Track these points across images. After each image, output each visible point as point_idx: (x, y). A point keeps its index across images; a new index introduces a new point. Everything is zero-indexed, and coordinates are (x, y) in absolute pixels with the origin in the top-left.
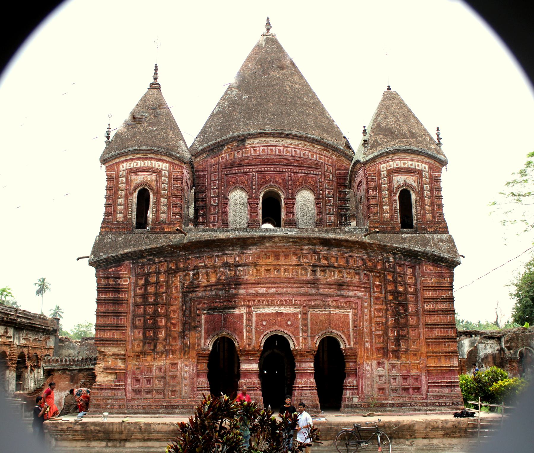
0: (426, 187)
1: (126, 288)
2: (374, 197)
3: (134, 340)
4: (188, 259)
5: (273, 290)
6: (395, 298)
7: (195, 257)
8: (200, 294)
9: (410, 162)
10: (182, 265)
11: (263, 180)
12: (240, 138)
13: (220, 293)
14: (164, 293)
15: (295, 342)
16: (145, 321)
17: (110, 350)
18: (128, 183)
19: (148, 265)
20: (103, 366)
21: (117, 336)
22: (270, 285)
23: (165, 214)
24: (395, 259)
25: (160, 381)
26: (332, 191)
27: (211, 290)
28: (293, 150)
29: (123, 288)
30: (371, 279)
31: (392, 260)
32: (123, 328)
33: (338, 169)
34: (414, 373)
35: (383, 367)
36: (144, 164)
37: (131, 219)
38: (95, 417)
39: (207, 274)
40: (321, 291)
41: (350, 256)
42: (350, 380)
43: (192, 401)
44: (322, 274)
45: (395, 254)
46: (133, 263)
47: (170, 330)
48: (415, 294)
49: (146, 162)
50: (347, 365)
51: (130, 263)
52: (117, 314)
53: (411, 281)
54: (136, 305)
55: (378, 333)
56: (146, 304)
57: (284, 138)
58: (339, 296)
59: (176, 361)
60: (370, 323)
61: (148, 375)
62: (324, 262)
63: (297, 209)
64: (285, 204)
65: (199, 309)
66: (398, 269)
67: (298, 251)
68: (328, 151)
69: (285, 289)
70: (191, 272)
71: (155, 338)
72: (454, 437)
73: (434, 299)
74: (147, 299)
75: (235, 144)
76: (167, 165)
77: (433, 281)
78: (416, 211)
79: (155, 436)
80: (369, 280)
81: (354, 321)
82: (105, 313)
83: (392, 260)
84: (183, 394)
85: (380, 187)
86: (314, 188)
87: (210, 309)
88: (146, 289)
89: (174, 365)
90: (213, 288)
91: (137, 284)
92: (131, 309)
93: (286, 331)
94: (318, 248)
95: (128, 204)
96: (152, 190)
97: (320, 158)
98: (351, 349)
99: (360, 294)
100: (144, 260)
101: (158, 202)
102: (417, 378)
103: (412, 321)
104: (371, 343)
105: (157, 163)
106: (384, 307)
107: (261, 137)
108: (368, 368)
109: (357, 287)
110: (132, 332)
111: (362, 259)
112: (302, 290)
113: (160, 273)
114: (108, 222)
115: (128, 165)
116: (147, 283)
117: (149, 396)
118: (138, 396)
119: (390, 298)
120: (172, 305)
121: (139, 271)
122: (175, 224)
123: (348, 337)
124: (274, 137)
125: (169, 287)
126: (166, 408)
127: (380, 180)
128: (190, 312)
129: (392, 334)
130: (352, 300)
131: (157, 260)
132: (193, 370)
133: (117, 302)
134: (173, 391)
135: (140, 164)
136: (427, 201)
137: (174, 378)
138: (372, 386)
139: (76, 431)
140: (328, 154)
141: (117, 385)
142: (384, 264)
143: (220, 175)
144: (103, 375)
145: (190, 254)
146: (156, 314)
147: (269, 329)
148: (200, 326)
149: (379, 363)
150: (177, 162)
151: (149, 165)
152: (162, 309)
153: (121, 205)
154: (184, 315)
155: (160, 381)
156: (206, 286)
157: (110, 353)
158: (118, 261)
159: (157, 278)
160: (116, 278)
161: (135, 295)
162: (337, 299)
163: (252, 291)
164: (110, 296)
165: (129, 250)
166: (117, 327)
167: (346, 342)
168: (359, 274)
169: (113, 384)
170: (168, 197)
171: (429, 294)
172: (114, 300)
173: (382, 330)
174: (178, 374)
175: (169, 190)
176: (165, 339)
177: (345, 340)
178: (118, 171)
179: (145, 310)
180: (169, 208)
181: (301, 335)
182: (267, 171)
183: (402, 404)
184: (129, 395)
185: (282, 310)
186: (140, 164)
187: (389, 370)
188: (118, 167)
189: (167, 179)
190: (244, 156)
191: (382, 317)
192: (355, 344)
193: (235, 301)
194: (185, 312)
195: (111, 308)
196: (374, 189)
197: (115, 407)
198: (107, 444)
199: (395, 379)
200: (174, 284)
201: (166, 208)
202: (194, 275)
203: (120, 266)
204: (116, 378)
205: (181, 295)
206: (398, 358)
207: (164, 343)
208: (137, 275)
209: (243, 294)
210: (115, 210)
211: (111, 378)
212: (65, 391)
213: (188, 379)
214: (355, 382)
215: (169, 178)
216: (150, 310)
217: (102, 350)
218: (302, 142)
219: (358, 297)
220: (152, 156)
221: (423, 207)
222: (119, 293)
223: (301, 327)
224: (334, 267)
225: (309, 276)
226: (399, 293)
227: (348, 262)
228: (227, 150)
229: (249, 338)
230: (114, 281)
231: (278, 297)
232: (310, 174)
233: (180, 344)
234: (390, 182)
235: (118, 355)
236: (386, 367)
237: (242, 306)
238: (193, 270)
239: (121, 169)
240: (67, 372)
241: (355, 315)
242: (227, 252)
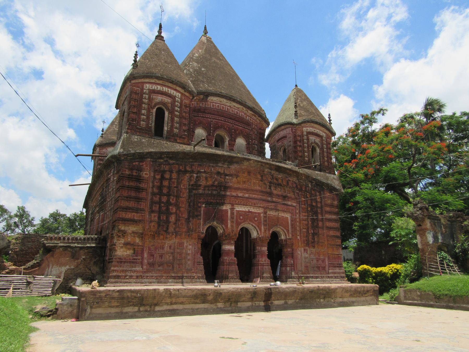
0: (325, 146)
1: (146, 180)
2: (300, 146)
3: (151, 222)
4: (193, 165)
5: (247, 195)
6: (311, 209)
7: (198, 165)
8: (201, 191)
9: (317, 130)
10: (188, 169)
11: (217, 126)
12: (206, 94)
13: (214, 192)
14: (175, 187)
15: (259, 232)
16: (160, 207)
17: (131, 229)
18: (150, 99)
19: (164, 165)
20: (123, 242)
21: (136, 216)
22: (245, 192)
23: (177, 129)
24: (311, 185)
25: (170, 256)
26: (256, 142)
27: (208, 190)
28: (236, 110)
29: (143, 180)
30: (300, 196)
31: (310, 186)
32: (143, 212)
33: (260, 129)
34: (322, 257)
35: (307, 253)
36: (163, 89)
37: (151, 127)
38: (117, 286)
39: (206, 178)
40: (274, 199)
41: (289, 180)
42: (289, 260)
43: (193, 272)
44: (274, 188)
45: (312, 182)
46: (153, 162)
47: (179, 217)
48: (322, 208)
49: (164, 88)
50: (285, 250)
51: (150, 161)
52: (138, 200)
53: (319, 200)
54: (153, 194)
55: (304, 230)
56: (161, 193)
57: (232, 101)
58: (284, 204)
59: (183, 241)
60: (300, 223)
61: (161, 251)
62: (275, 181)
63: (235, 148)
64: (229, 144)
65: (200, 202)
66: (313, 192)
67: (261, 172)
68: (255, 116)
69: (254, 196)
70: (195, 175)
71: (168, 222)
72: (354, 297)
73: (330, 213)
74: (162, 190)
75: (202, 96)
76: (180, 95)
77: (329, 202)
78: (320, 159)
79: (181, 299)
80: (298, 196)
81: (292, 221)
82: (127, 197)
83: (310, 186)
84: (187, 267)
85: (303, 140)
86: (247, 137)
87: (208, 203)
88: (161, 183)
89: (181, 244)
90: (210, 188)
91: (156, 178)
92: (149, 197)
93: (254, 225)
94: (273, 172)
95: (150, 116)
96: (168, 109)
97: (250, 120)
98: (290, 239)
99: (294, 204)
100: (162, 161)
101: (172, 120)
102: (323, 261)
103: (320, 224)
104: (301, 236)
105: (172, 91)
106: (306, 214)
107: (218, 96)
108: (299, 253)
109: (293, 200)
110: (150, 215)
111: (295, 183)
112: (264, 198)
113: (173, 173)
114: (133, 126)
115: (150, 86)
116: (163, 178)
117: (161, 268)
118: (152, 268)
119: (309, 209)
120: (181, 197)
121: (157, 168)
122: (184, 138)
123: (288, 231)
124: (226, 99)
125: (179, 183)
126: (174, 279)
127: (303, 137)
128: (194, 204)
129: (311, 231)
130: (291, 207)
131: (171, 162)
132: (195, 248)
133: (138, 189)
134: (179, 265)
135: (159, 88)
136: (325, 154)
137: (181, 254)
138: (301, 264)
139: (113, 298)
140: (255, 118)
141: (135, 259)
142: (306, 188)
143: (191, 116)
144: (122, 250)
145: (195, 162)
146: (168, 203)
147: (244, 222)
148: (200, 215)
149: (305, 250)
150: (187, 94)
151: (167, 91)
152: (173, 200)
153: (144, 115)
154: (189, 206)
155: (170, 256)
156: (205, 187)
157: (130, 231)
158: (142, 157)
159: (171, 175)
160: (139, 171)
161: (153, 186)
162: (283, 206)
163: (234, 194)
164: (132, 184)
165: (152, 150)
166: (137, 210)
167: (287, 235)
168: (294, 192)
169: (131, 258)
170: (181, 117)
171: (328, 209)
172: (136, 188)
173: (305, 229)
174: (184, 251)
175: (180, 112)
176: (175, 224)
177: (287, 233)
178: (143, 89)
179: (160, 199)
180: (180, 126)
181: (262, 227)
182: (220, 120)
183: (317, 277)
184: (145, 267)
185: (252, 210)
186: (159, 88)
187: (310, 254)
188: (143, 86)
189: (179, 105)
190: (206, 106)
191: (305, 220)
192: (293, 235)
193: (224, 200)
194: (190, 203)
195: (133, 194)
196: (300, 141)
197: (134, 277)
198: (139, 309)
199: (312, 260)
200: (183, 182)
201: (178, 125)
202: (197, 177)
203: (143, 162)
204: (134, 253)
205: (188, 190)
206: (314, 247)
207: (174, 226)
208: (155, 171)
209: (228, 196)
210: (139, 118)
211: (129, 252)
212: (65, 266)
213: (190, 255)
214: (292, 262)
215: (181, 103)
216: (164, 199)
217: (123, 228)
218: (241, 107)
219: (294, 206)
220: (170, 85)
221: (323, 157)
222: (140, 183)
223: (262, 222)
224: (281, 185)
225: (268, 190)
226: (313, 206)
227: (288, 183)
228: (195, 100)
229: (232, 226)
230: (136, 173)
231: (250, 200)
232: (245, 128)
233: (186, 227)
234: (308, 139)
235: (136, 233)
236: (308, 252)
237: (228, 204)
238: (197, 174)
239: (145, 88)
240: (69, 249)
241: (291, 217)
242: (219, 165)
